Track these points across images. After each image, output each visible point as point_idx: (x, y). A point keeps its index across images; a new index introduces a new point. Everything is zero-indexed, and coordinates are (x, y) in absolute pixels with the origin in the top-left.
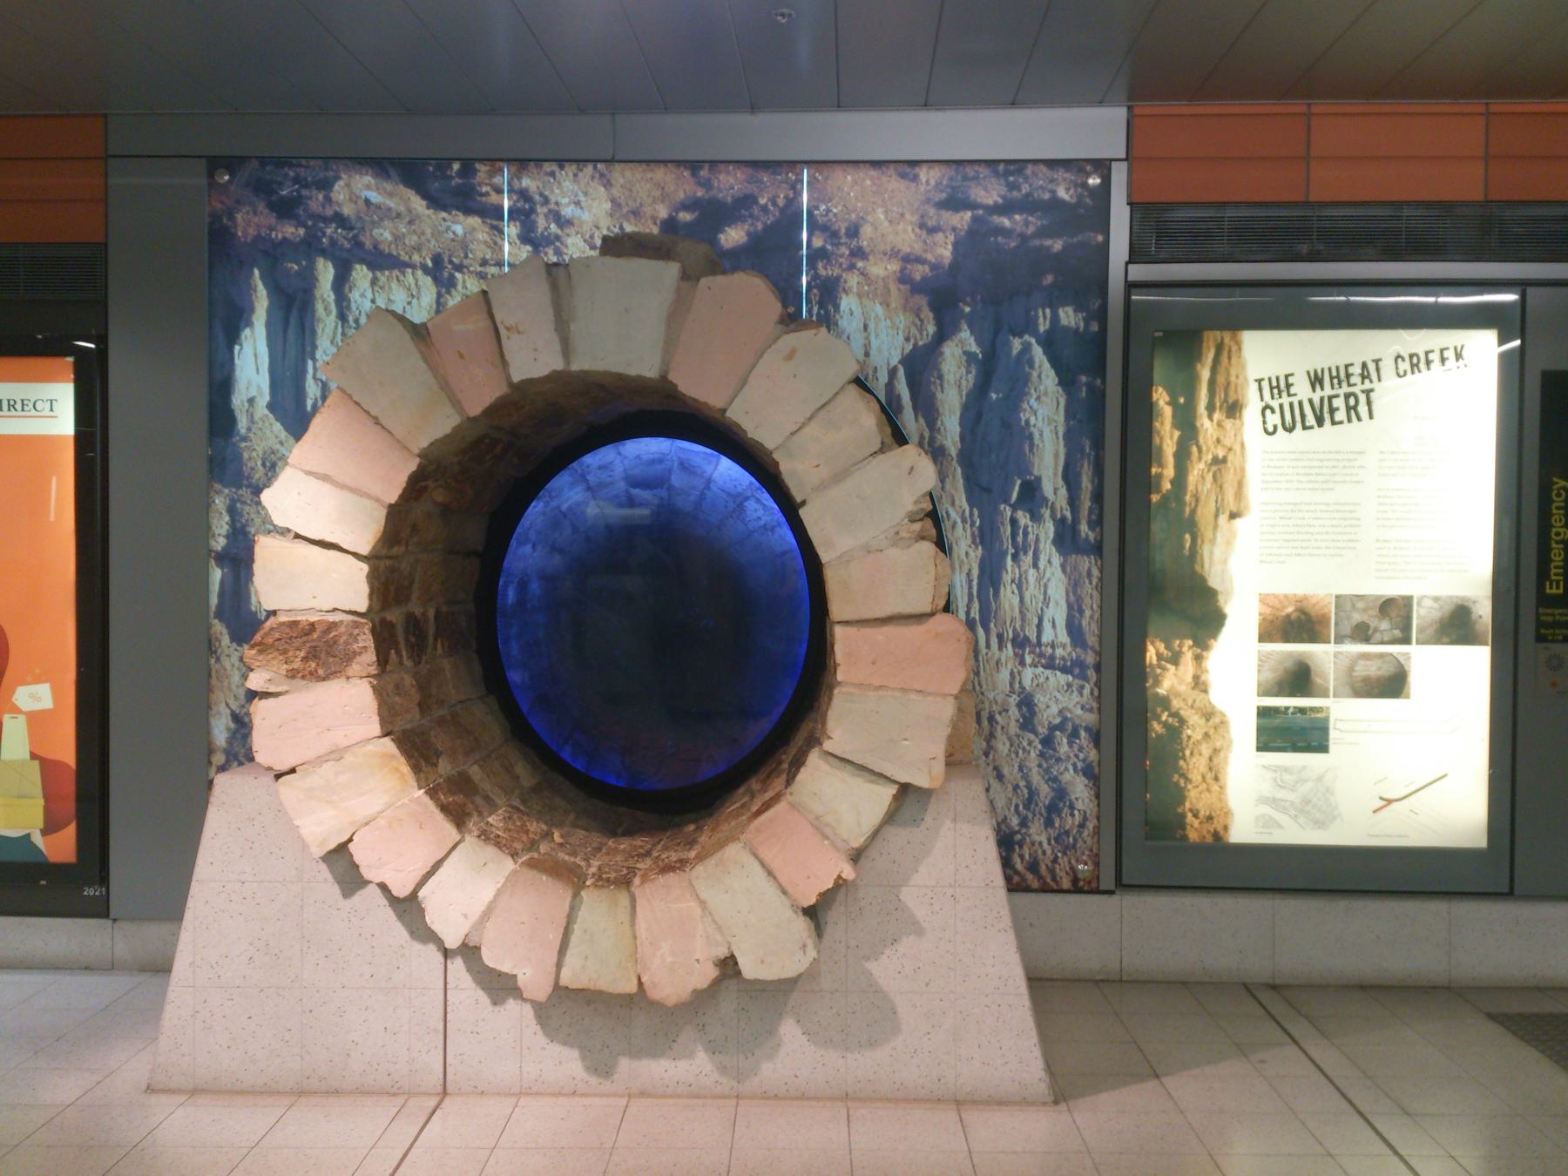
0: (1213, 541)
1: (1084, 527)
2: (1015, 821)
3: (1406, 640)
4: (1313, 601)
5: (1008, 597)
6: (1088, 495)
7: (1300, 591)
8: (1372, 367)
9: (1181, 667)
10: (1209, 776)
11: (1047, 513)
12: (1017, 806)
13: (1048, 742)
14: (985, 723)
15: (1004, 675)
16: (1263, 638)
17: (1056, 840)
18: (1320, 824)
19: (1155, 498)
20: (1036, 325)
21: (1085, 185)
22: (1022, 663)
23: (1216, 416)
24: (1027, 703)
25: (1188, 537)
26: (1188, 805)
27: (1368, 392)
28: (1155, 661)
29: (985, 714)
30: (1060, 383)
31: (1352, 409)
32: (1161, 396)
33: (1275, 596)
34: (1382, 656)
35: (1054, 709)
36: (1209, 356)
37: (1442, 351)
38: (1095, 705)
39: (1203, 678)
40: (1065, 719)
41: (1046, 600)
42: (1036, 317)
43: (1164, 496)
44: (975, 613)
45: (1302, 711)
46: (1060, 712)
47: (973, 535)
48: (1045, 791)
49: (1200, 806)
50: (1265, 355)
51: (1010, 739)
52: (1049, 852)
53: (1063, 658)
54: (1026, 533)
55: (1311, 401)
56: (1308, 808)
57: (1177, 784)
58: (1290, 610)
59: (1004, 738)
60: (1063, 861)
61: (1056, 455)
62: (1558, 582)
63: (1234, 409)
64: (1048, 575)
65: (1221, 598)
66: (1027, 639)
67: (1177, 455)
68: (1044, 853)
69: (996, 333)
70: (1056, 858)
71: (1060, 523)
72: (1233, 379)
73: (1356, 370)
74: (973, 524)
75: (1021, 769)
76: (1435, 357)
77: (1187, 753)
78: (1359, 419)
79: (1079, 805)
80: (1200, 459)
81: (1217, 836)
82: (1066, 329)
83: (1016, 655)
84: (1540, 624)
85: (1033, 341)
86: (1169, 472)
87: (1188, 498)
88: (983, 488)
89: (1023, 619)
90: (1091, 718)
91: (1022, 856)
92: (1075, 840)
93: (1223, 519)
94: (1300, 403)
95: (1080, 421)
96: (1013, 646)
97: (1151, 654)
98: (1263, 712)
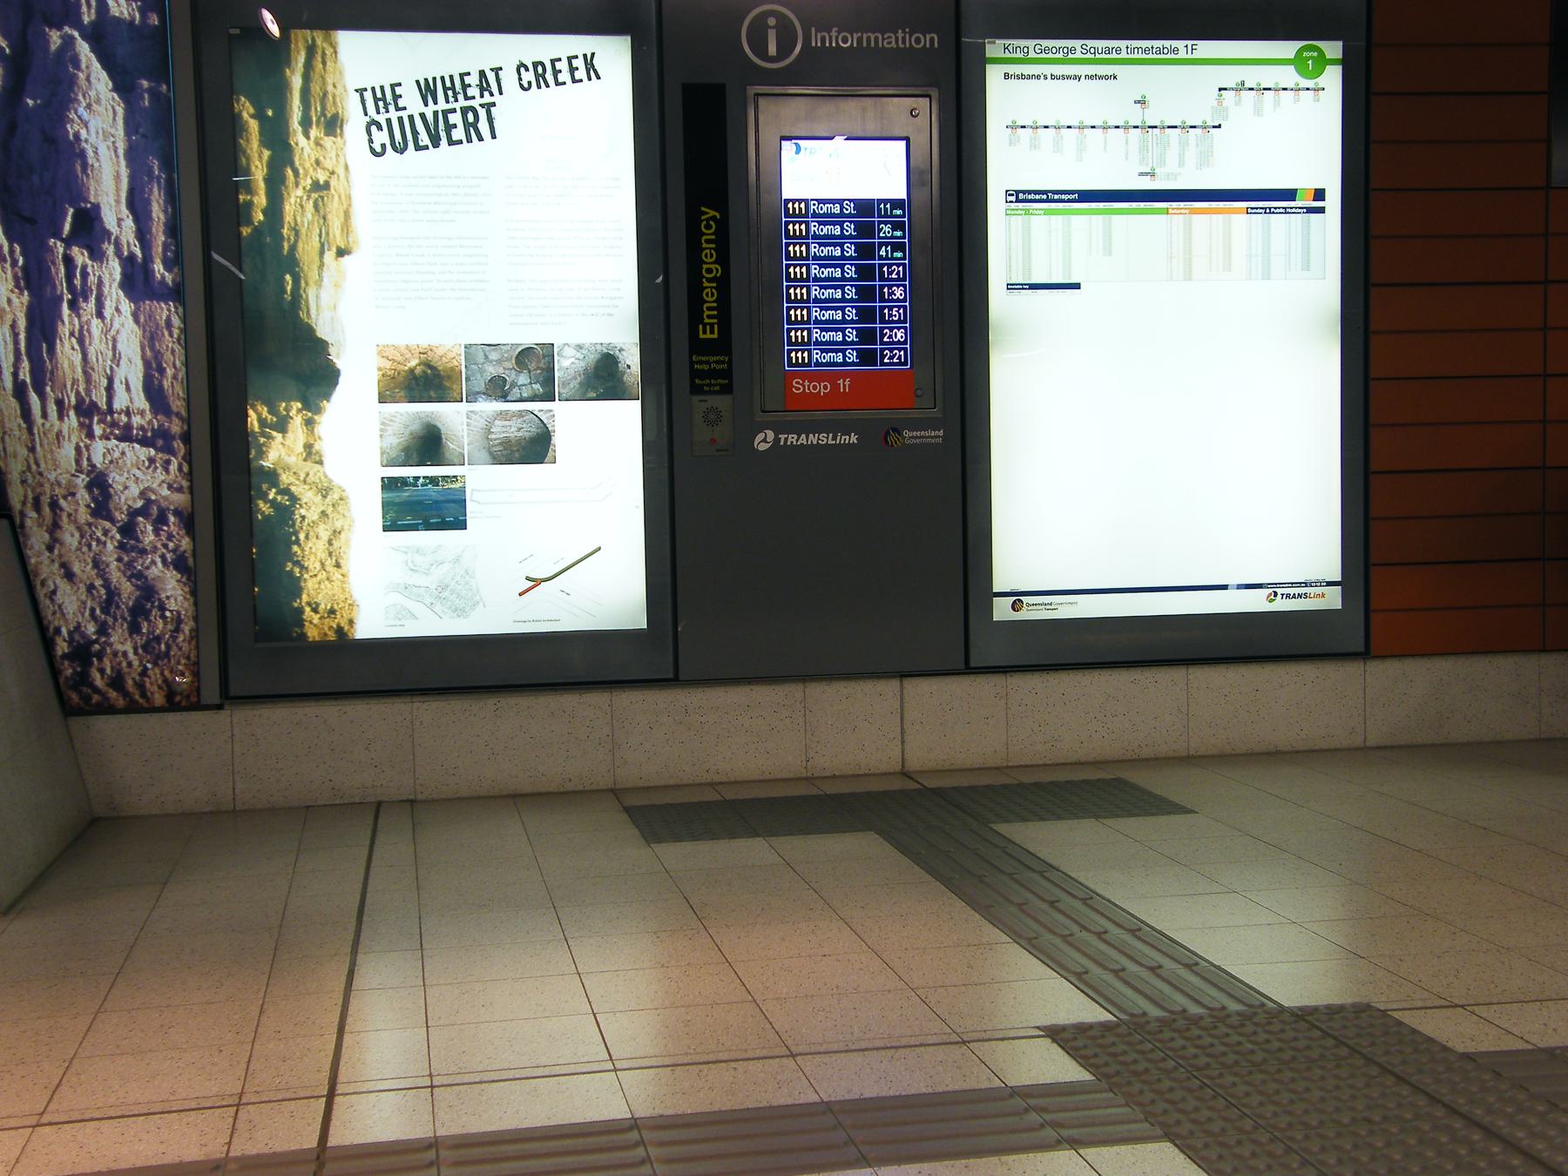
0: (319, 283)
1: (158, 267)
2: (91, 629)
3: (550, 397)
4: (440, 352)
5: (67, 354)
6: (161, 228)
7: (424, 342)
8: (491, 77)
9: (290, 435)
10: (329, 563)
11: (110, 250)
12: (93, 610)
13: (128, 530)
14: (47, 510)
15: (68, 451)
16: (382, 399)
17: (144, 647)
18: (459, 612)
19: (246, 231)
20: (79, 15)
22: (90, 435)
23: (314, 132)
24: (99, 483)
25: (288, 277)
26: (305, 598)
27: (489, 107)
28: (257, 429)
29: (45, 500)
30: (116, 89)
31: (471, 127)
32: (246, 109)
33: (395, 348)
34: (521, 414)
35: (135, 490)
36: (300, 59)
37: (570, 59)
38: (185, 484)
39: (317, 447)
40: (149, 502)
41: (116, 358)
43: (256, 229)
44: (25, 375)
45: (433, 480)
46: (142, 494)
47: (15, 277)
48: (127, 589)
49: (320, 598)
50: (366, 59)
51: (79, 529)
52: (136, 663)
53: (142, 428)
54: (85, 275)
55: (423, 116)
56: (444, 595)
57: (291, 572)
58: (414, 363)
59: (72, 528)
60: (155, 673)
61: (117, 177)
62: (712, 325)
63: (333, 125)
64: (116, 325)
65: (332, 350)
66: (94, 405)
67: (267, 181)
68: (130, 665)
70: (146, 669)
71: (128, 262)
72: (330, 88)
73: (473, 80)
74: (14, 263)
75: (96, 564)
76: (563, 65)
77: (302, 536)
78: (481, 139)
79: (172, 605)
80: (297, 185)
81: (340, 631)
82: (118, 21)
83: (81, 425)
84: (694, 374)
85: (76, 34)
86: (261, 200)
87: (285, 231)
88: (26, 219)
89: (88, 380)
90: (181, 499)
91: (102, 671)
92: (168, 647)
93: (329, 256)
94: (411, 118)
95: (144, 136)
96: (78, 414)
97: (253, 417)
98: (389, 484)
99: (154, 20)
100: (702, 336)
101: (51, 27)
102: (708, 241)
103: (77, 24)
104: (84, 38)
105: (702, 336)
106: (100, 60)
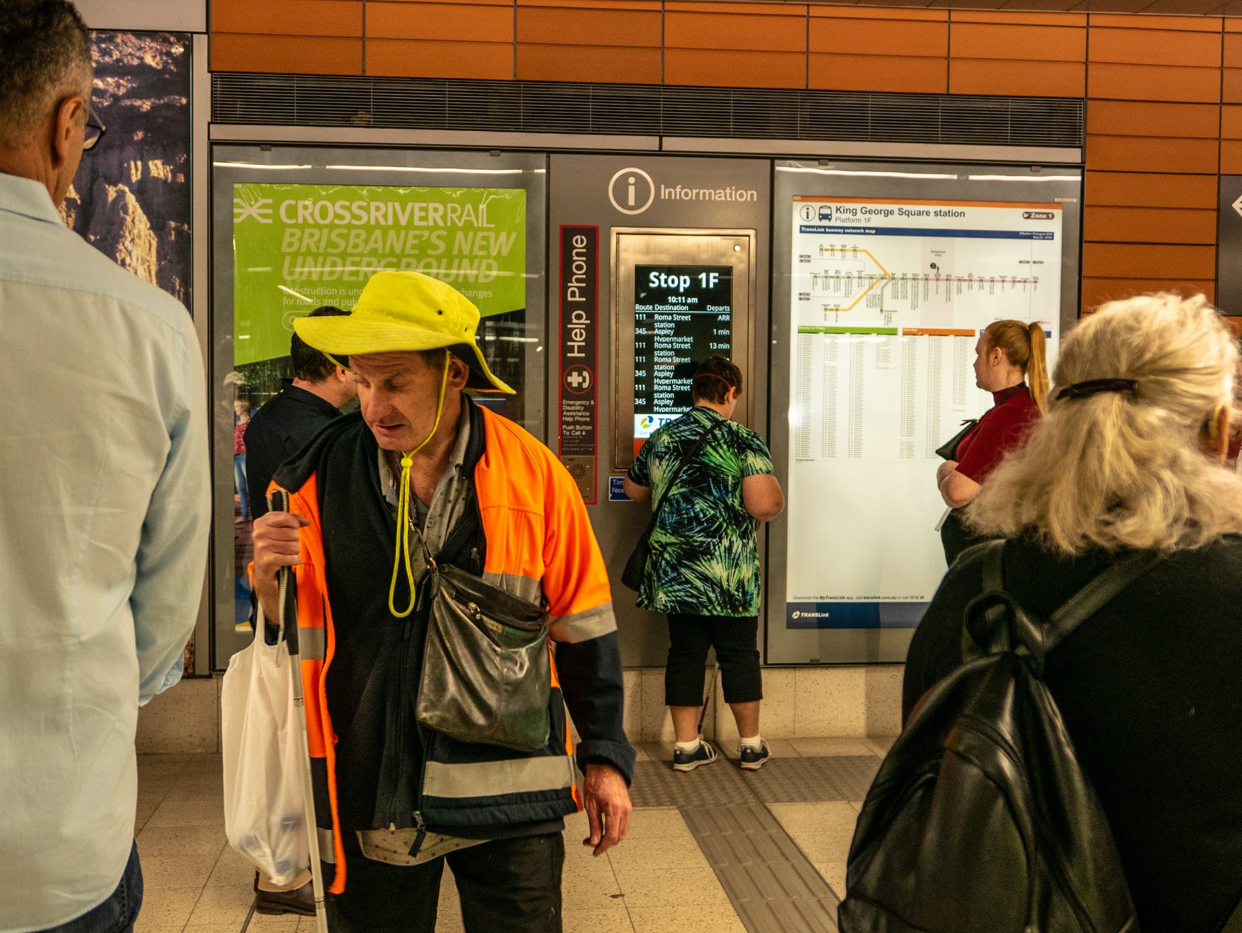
21: (169, 54)
30: (152, 228)
42: (129, 166)
69: (93, 180)
82: (156, 179)
85: (126, 189)
95: (170, 261)
99: (181, 178)
100: (570, 299)
101: (110, 184)
102: (578, 254)
103: (128, 182)
104: (132, 192)
105: (570, 299)
106: (143, 207)
